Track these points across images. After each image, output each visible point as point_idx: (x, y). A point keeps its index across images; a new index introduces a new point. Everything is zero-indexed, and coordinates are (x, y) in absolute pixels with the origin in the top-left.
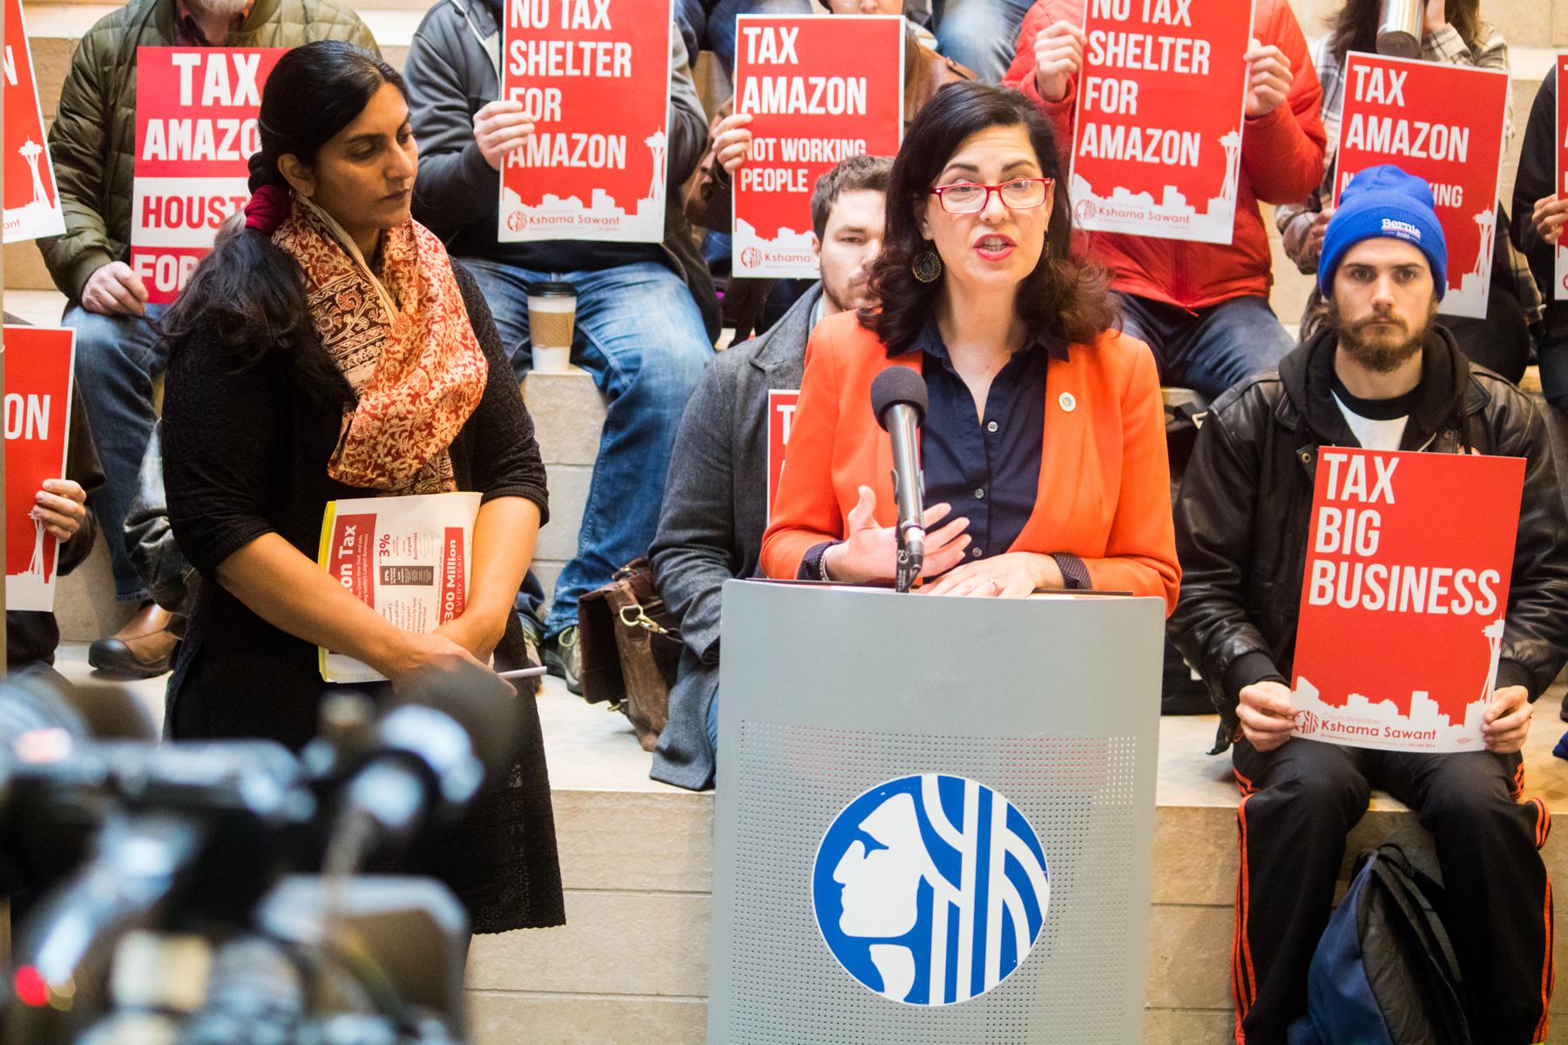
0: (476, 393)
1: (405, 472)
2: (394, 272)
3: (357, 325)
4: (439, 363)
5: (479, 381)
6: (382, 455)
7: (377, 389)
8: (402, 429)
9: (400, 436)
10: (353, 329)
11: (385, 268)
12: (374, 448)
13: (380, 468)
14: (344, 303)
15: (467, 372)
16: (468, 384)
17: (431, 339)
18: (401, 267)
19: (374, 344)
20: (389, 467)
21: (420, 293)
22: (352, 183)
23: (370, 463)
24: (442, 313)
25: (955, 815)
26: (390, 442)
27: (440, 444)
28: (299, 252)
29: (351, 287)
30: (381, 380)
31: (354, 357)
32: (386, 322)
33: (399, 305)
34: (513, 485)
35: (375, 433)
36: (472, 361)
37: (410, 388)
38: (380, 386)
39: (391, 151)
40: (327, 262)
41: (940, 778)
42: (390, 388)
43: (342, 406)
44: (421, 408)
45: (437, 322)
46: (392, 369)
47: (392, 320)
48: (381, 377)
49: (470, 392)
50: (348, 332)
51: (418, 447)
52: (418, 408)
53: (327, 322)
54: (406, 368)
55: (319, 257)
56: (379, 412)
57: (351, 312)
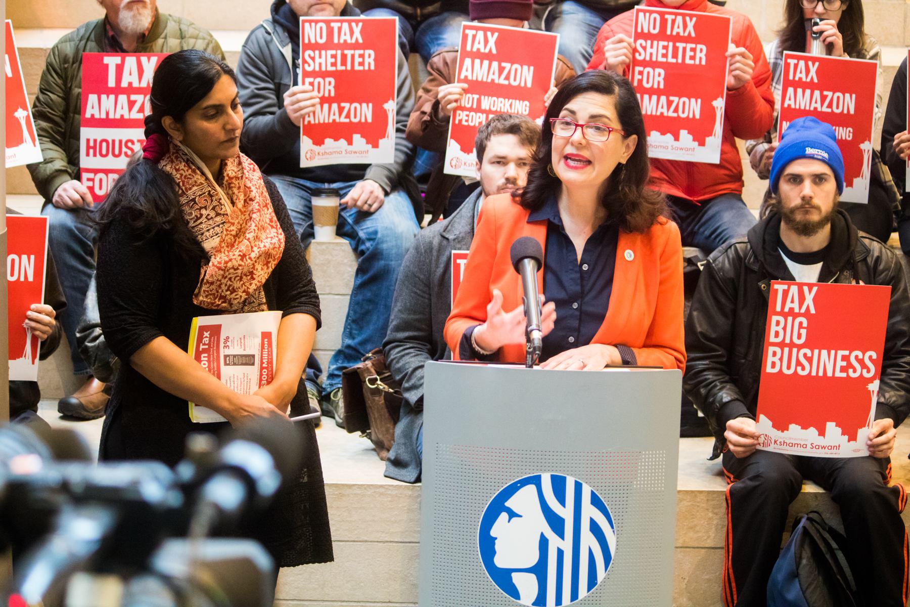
0: (278, 253)
1: (238, 300)
2: (230, 184)
3: (208, 215)
4: (257, 237)
5: (280, 247)
6: (224, 291)
7: (221, 252)
8: (236, 275)
10: (206, 218)
11: (225, 182)
12: (220, 286)
13: (223, 298)
14: (201, 202)
15: (273, 241)
16: (274, 248)
17: (252, 222)
18: (234, 181)
20: (228, 297)
21: (245, 195)
22: (205, 133)
23: (217, 295)
24: (257, 207)
25: (560, 496)
26: (229, 283)
28: (174, 173)
29: (205, 193)
30: (223, 247)
31: (207, 234)
32: (226, 213)
33: (233, 203)
34: (300, 306)
35: (220, 278)
36: (276, 234)
37: (240, 251)
38: (223, 250)
39: (227, 114)
40: (191, 179)
41: (552, 476)
42: (228, 251)
43: (200, 262)
46: (229, 240)
47: (229, 212)
50: (203, 219)
51: (245, 286)
52: (245, 263)
53: (191, 214)
54: (237, 239)
55: (185, 176)
56: (222, 265)
57: (205, 208)
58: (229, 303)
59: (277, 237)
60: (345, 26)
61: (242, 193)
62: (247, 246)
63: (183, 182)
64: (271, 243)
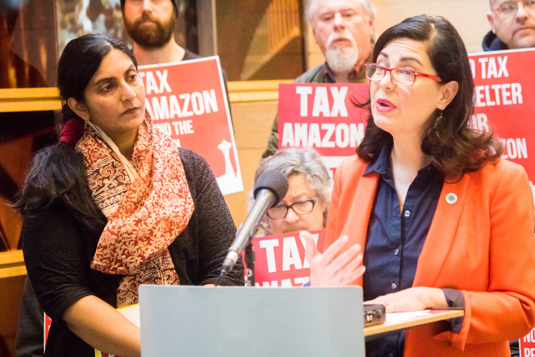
1: (134, 264)
2: (139, 157)
3: (111, 184)
4: (157, 204)
6: (120, 255)
7: (118, 217)
8: (129, 239)
9: (129, 243)
10: (108, 187)
12: (114, 250)
15: (177, 210)
16: (176, 217)
18: (143, 154)
19: (120, 194)
22: (103, 107)
23: (113, 259)
24: (161, 177)
26: (123, 247)
27: (154, 249)
29: (109, 165)
30: (121, 213)
34: (215, 277)
35: (113, 242)
36: (183, 204)
37: (136, 217)
38: (120, 216)
39: (122, 86)
40: (96, 152)
42: (126, 217)
44: (142, 228)
45: (157, 181)
46: (129, 207)
48: (121, 210)
49: (178, 221)
50: (105, 188)
51: (141, 250)
52: (139, 228)
53: (94, 184)
55: (93, 150)
56: (116, 231)
57: (108, 178)
58: (126, 267)
59: (184, 206)
61: (147, 164)
62: (144, 212)
63: (90, 155)
64: (173, 212)
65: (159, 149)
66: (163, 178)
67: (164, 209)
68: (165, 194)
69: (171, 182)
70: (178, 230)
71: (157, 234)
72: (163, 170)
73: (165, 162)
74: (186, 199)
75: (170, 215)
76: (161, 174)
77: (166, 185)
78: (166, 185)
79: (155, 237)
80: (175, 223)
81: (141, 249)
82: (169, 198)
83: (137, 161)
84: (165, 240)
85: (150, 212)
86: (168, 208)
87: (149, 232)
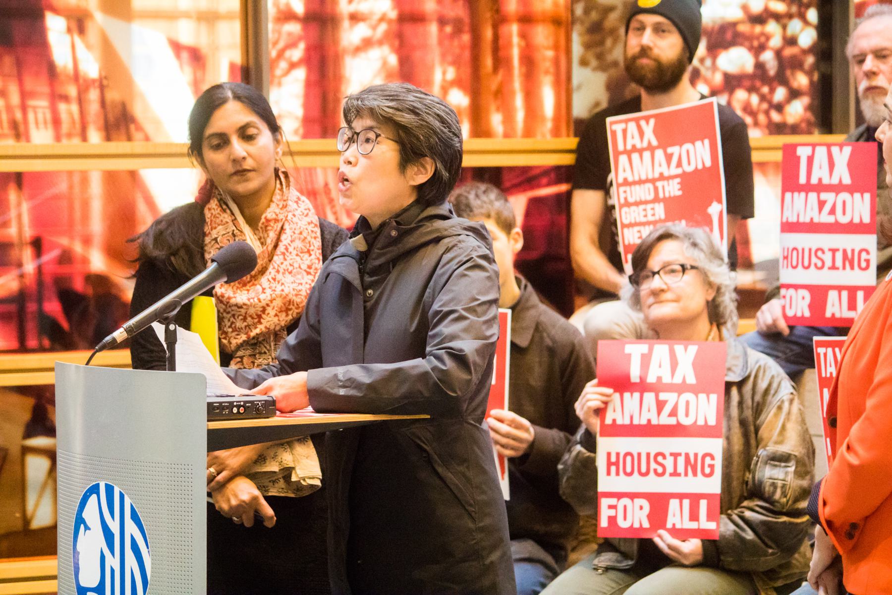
4: (274, 279)
15: (300, 287)
16: (296, 295)
54: (253, 281)
60: (632, 126)
63: (211, 221)
64: (294, 289)
65: (292, 218)
66: (287, 251)
67: (283, 286)
68: (288, 270)
69: (300, 256)
70: (297, 311)
71: (270, 313)
72: (290, 243)
73: (294, 233)
74: (314, 277)
75: (290, 293)
76: (285, 247)
77: (291, 259)
78: (291, 259)
79: (267, 316)
80: (295, 302)
81: (250, 327)
82: (292, 274)
83: (264, 231)
84: (279, 320)
85: (264, 287)
86: (289, 285)
87: (261, 309)
